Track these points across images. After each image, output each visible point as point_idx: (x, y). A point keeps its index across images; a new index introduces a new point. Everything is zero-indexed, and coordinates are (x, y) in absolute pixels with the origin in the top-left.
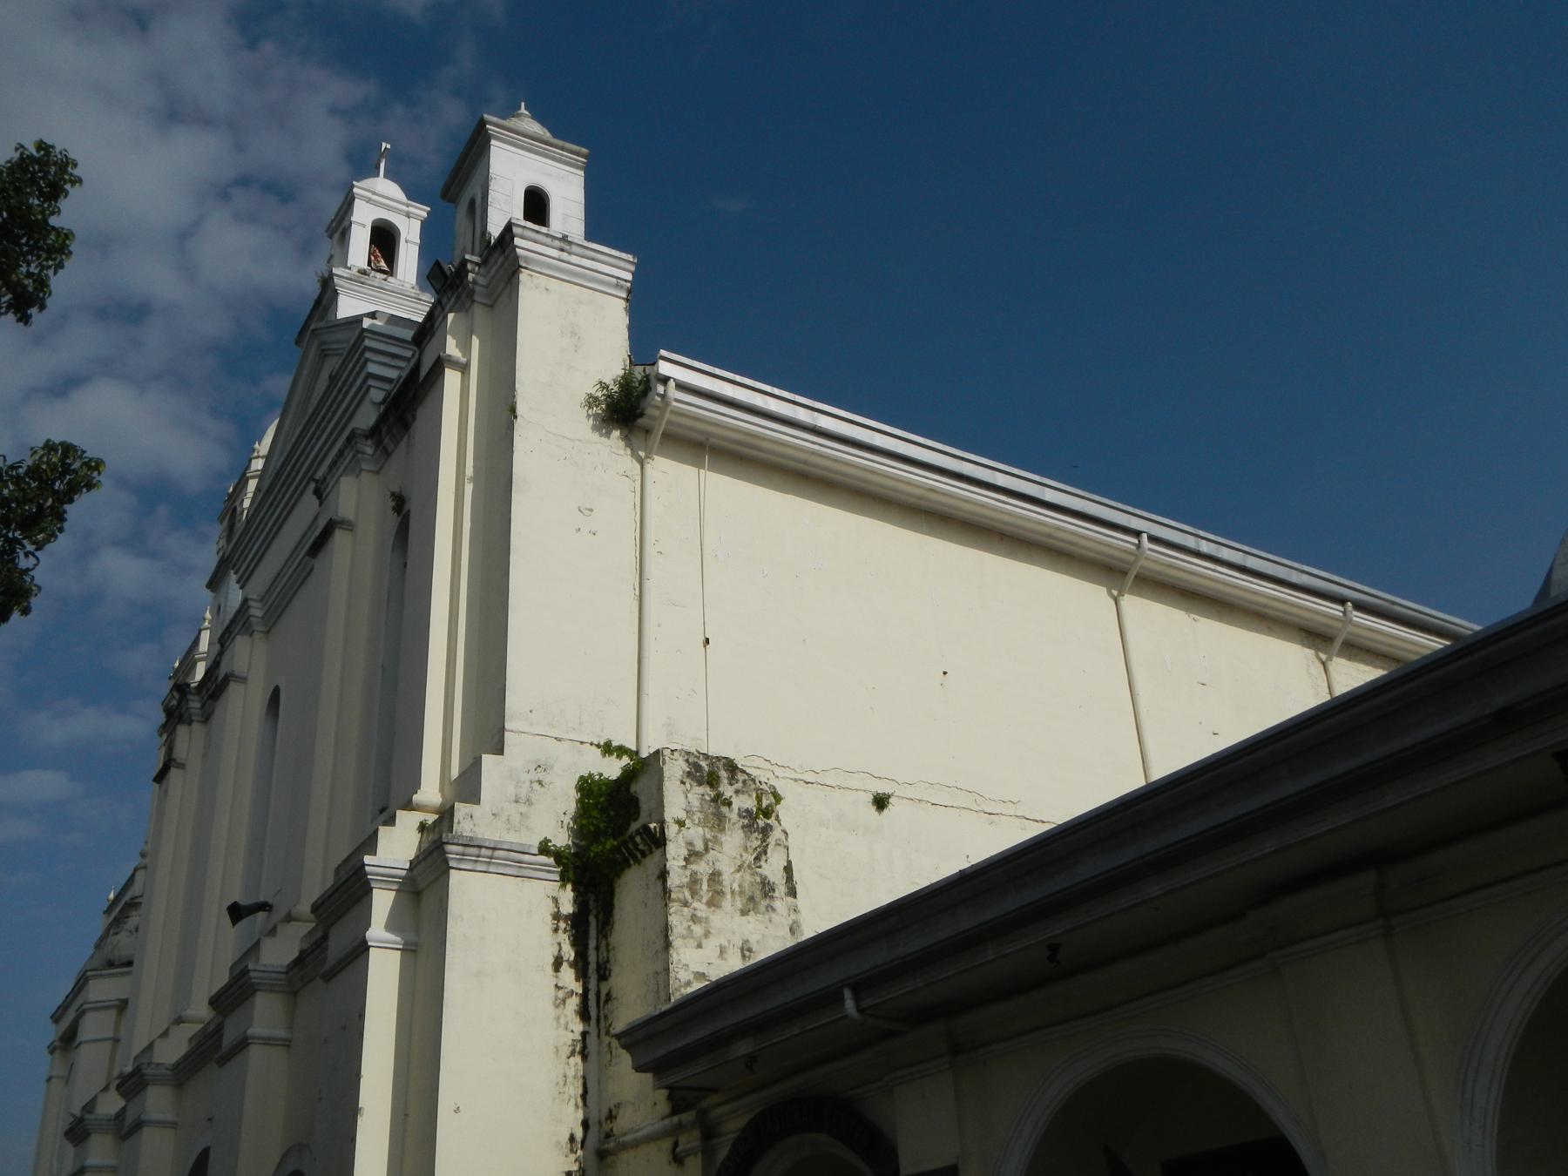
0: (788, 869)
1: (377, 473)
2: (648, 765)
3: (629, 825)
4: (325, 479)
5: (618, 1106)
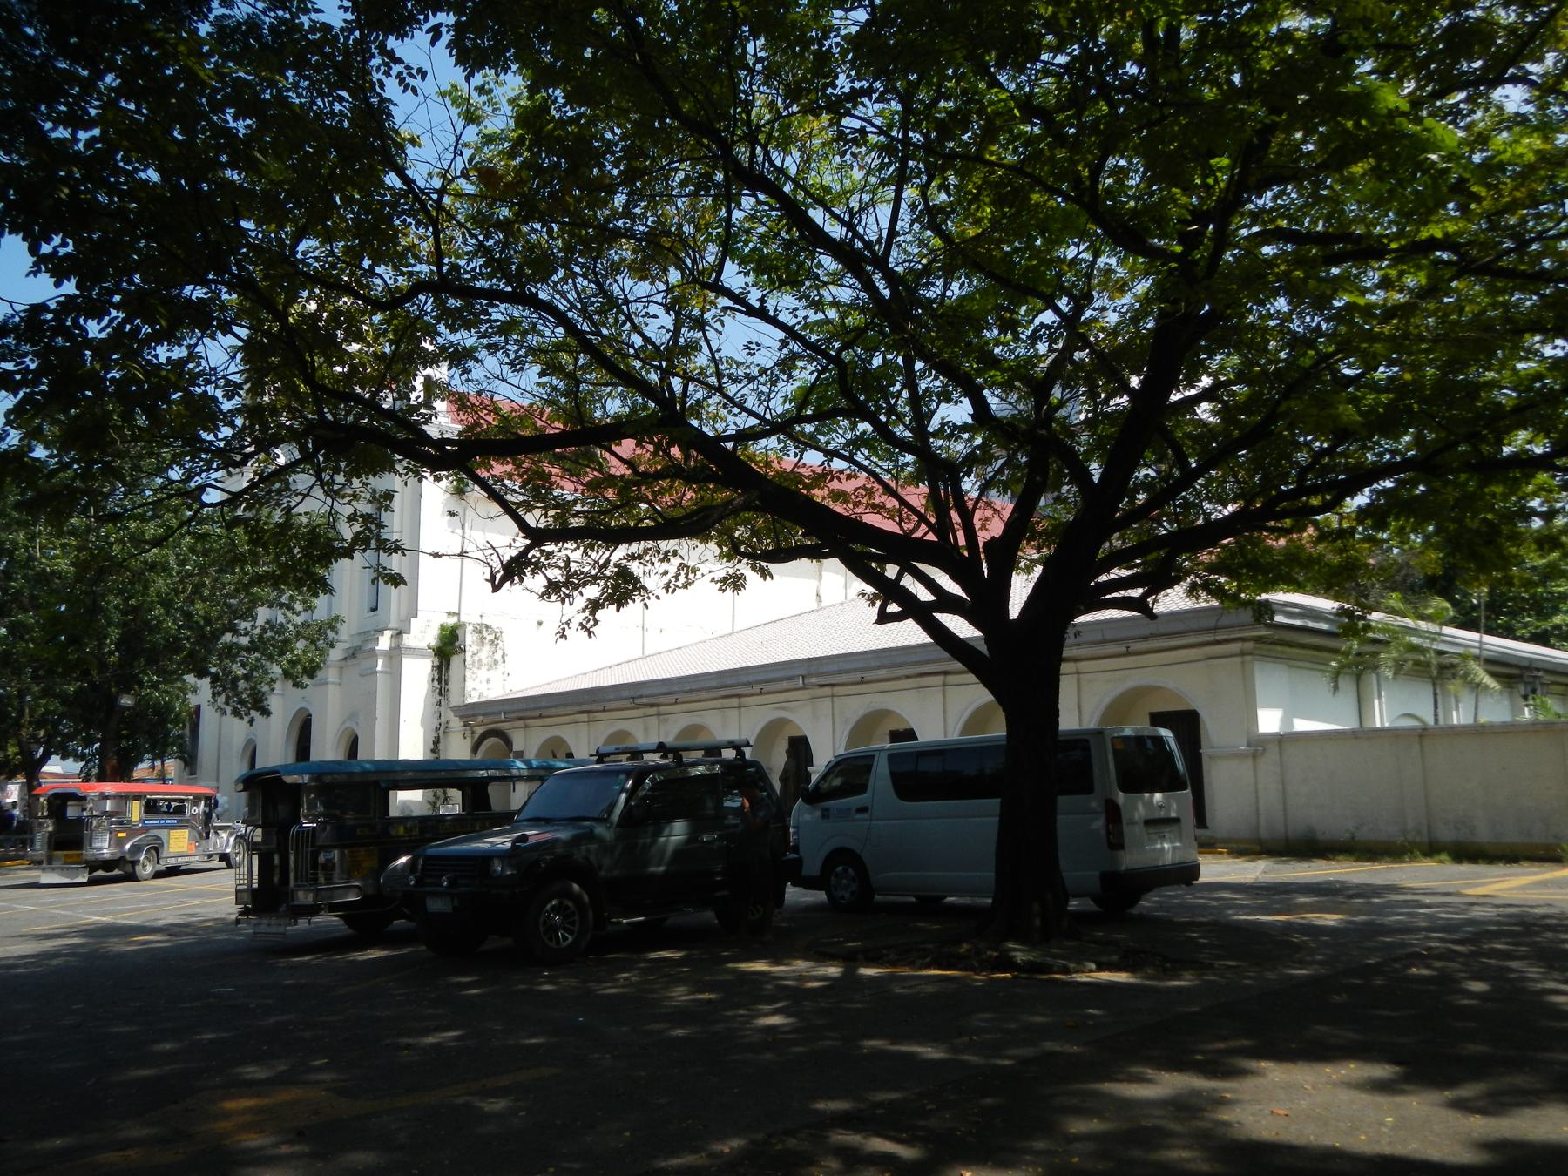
0: (503, 656)
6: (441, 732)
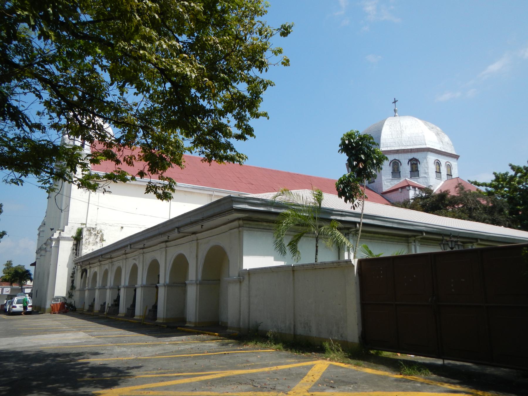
6: (76, 270)
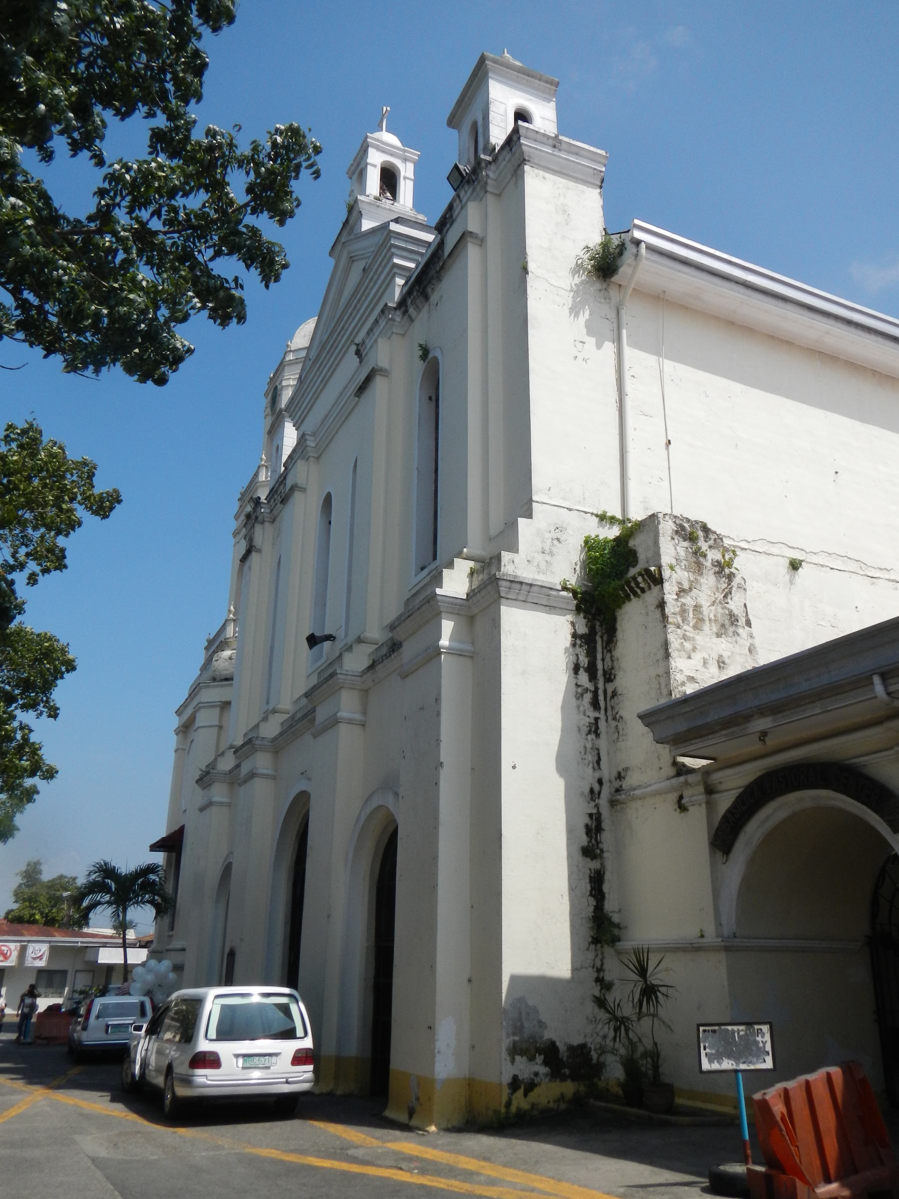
1: (403, 335)
2: (644, 526)
3: (627, 570)
4: (364, 342)
5: (626, 769)
